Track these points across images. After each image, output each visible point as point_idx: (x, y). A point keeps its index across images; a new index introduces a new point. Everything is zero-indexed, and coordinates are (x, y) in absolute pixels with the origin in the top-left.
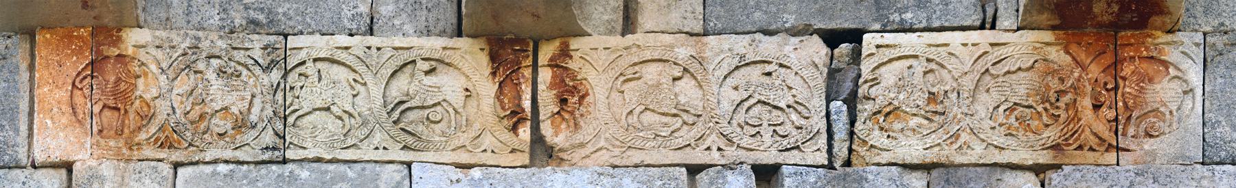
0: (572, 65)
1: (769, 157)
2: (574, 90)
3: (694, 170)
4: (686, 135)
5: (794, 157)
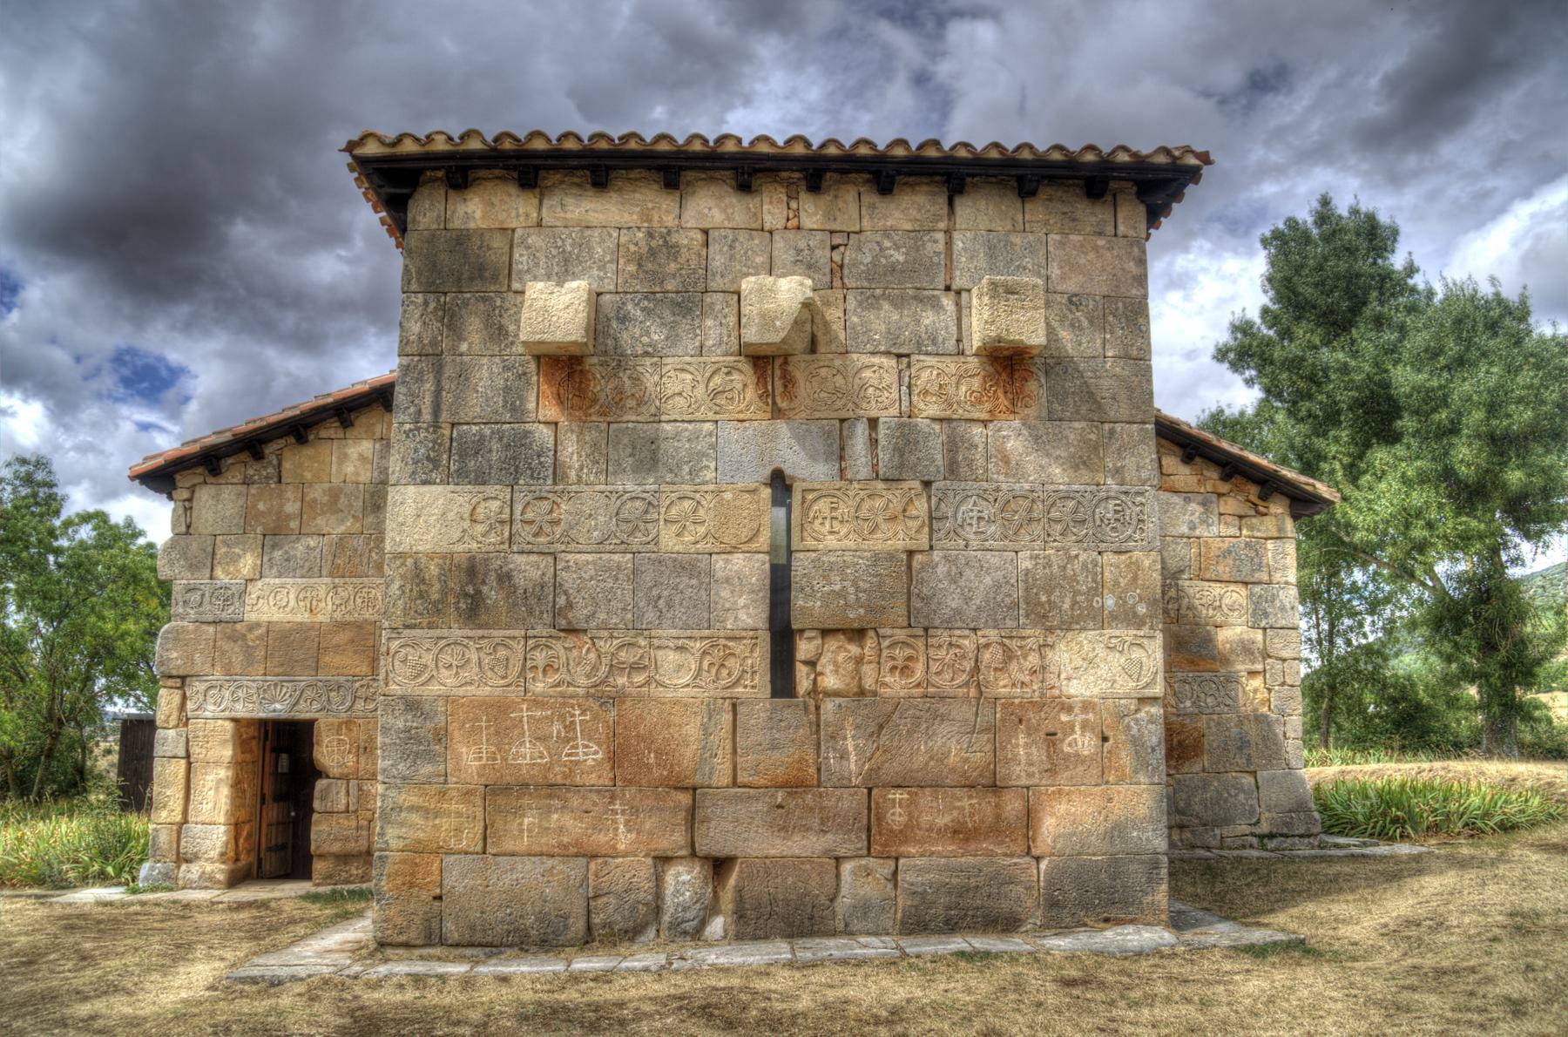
0: (790, 368)
1: (873, 414)
2: (790, 381)
3: (842, 421)
4: (839, 403)
5: (885, 413)
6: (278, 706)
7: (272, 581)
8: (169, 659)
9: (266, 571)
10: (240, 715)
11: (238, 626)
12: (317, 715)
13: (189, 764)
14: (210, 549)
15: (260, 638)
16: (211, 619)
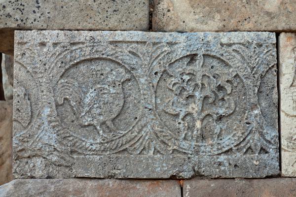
16: (162, 169)
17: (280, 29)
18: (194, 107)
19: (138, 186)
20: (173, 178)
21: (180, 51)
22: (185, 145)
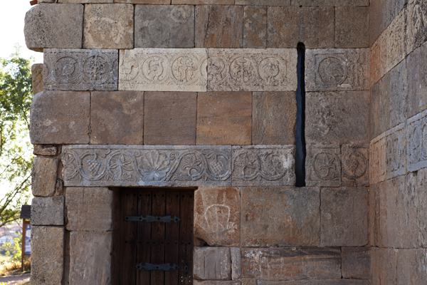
6: (157, 175)
7: (146, 51)
8: (44, 128)
9: (139, 41)
10: (117, 184)
11: (114, 96)
12: (197, 184)
13: (67, 232)
14: (79, 18)
15: (136, 106)
16: (84, 88)
17: (119, 48)
18: (94, 71)
19: (79, 93)
20: (88, 91)
21: (90, 55)
22: (91, 81)
